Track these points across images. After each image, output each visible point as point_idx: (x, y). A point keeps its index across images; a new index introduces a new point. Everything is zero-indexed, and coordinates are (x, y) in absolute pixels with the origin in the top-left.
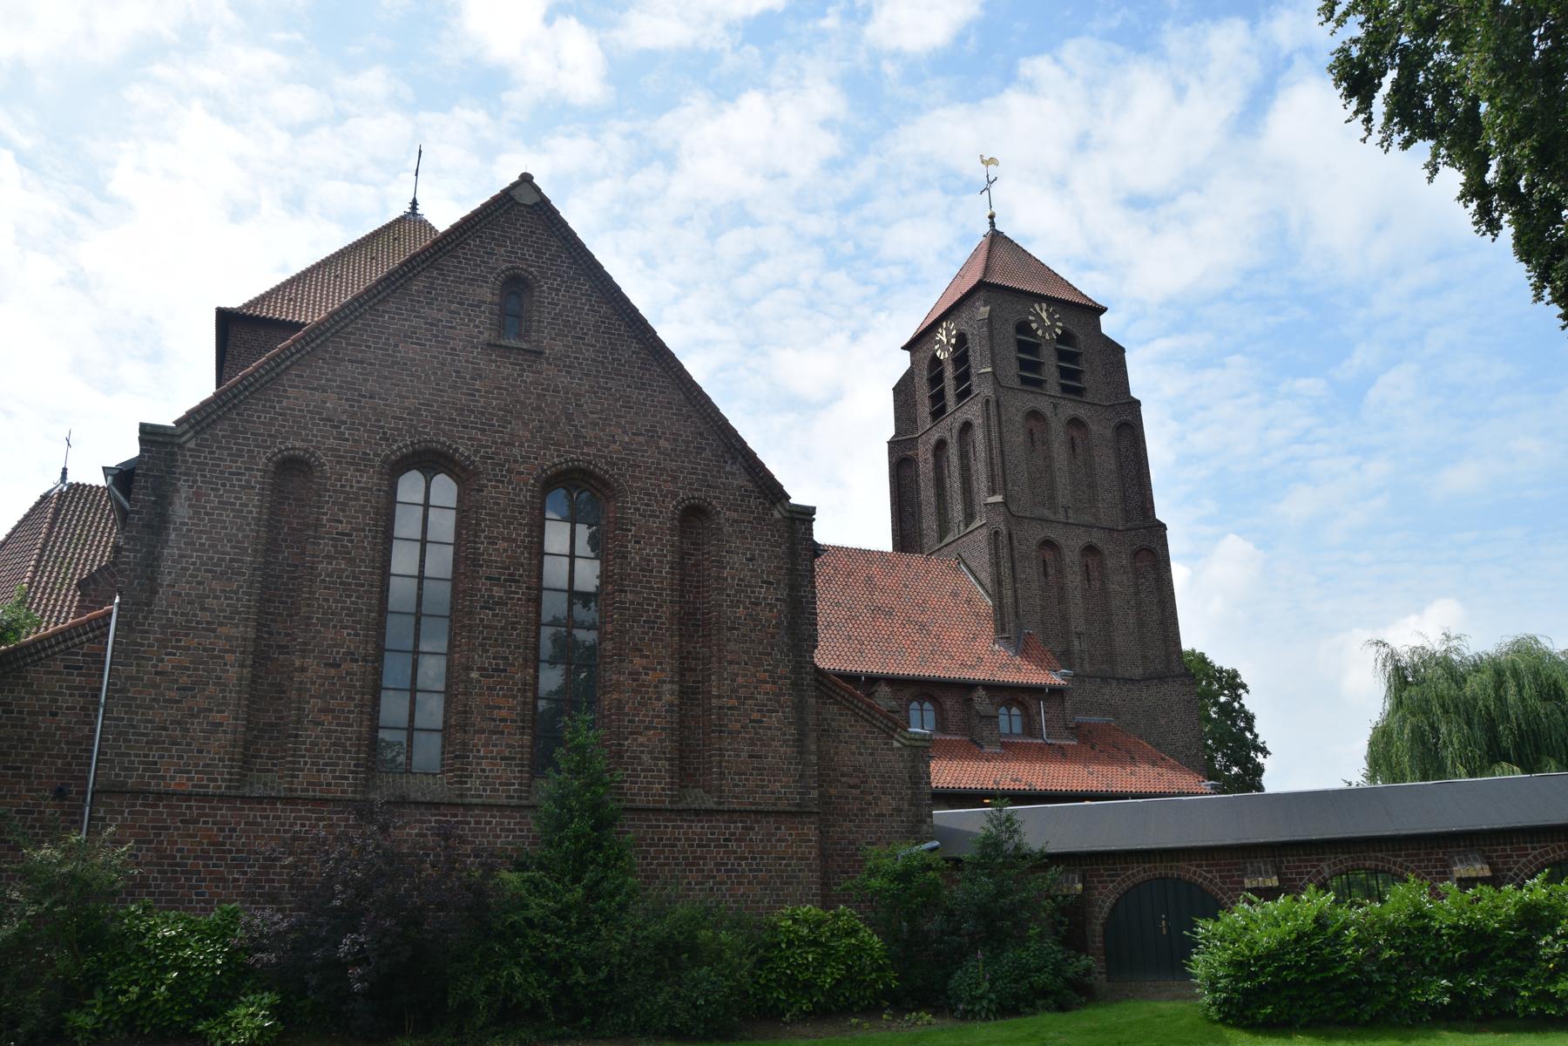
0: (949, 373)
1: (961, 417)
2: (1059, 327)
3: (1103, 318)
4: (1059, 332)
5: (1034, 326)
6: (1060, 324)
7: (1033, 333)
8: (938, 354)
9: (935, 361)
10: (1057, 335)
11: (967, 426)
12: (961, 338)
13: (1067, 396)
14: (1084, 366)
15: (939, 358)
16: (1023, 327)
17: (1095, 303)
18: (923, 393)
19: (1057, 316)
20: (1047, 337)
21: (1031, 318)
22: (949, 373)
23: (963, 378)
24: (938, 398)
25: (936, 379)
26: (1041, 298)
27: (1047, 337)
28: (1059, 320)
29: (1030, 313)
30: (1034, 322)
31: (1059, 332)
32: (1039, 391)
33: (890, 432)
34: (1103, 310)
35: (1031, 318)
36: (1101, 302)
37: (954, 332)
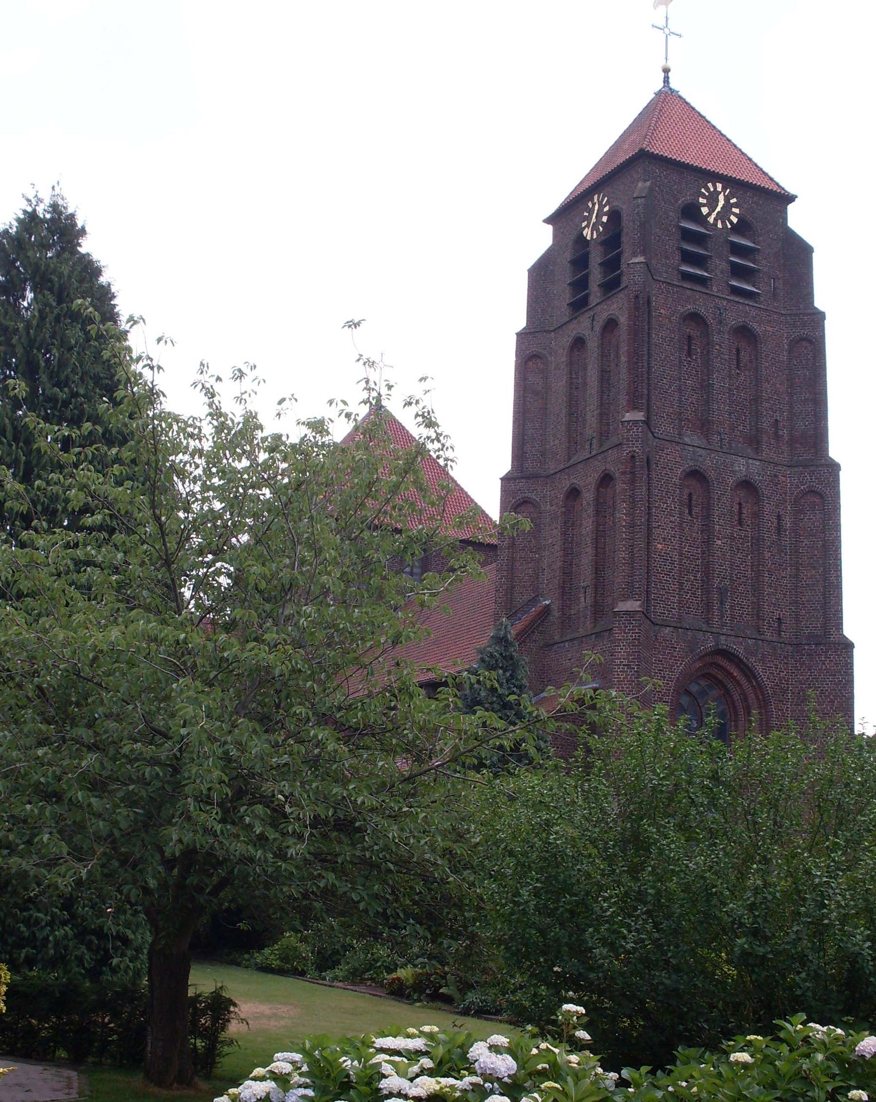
0: (596, 258)
1: (603, 313)
2: (735, 215)
3: (791, 208)
4: (735, 220)
5: (705, 210)
6: (736, 210)
7: (702, 220)
8: (585, 233)
9: (581, 240)
10: (731, 222)
11: (611, 324)
12: (615, 216)
13: (737, 299)
14: (761, 264)
15: (585, 238)
16: (691, 212)
17: (783, 189)
18: (564, 276)
19: (733, 201)
20: (720, 225)
21: (701, 200)
22: (596, 258)
23: (612, 264)
24: (580, 285)
25: (581, 262)
26: (715, 177)
27: (720, 225)
28: (736, 205)
29: (704, 196)
30: (704, 205)
31: (735, 220)
32: (704, 290)
33: (520, 321)
34: (791, 199)
35: (701, 200)
36: (790, 189)
37: (606, 209)
